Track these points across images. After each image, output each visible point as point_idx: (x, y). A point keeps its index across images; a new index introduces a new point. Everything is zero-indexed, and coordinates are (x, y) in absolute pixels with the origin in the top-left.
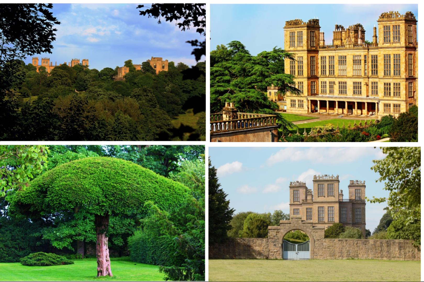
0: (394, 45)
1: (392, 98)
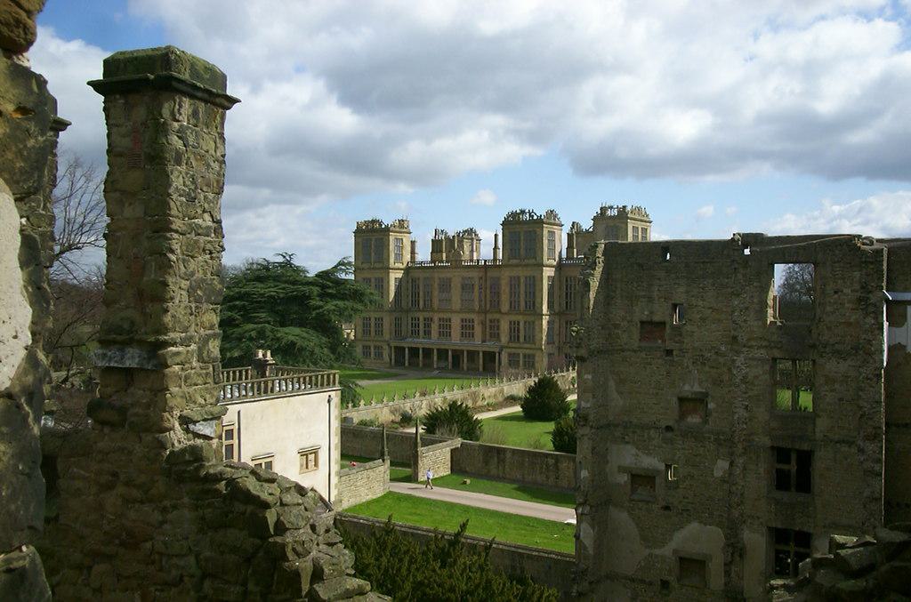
1: (522, 346)
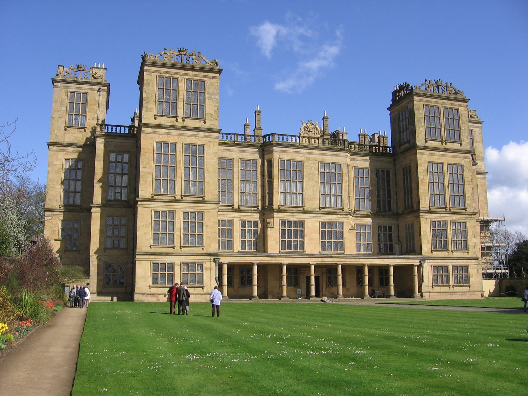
0: (449, 145)
1: (450, 255)
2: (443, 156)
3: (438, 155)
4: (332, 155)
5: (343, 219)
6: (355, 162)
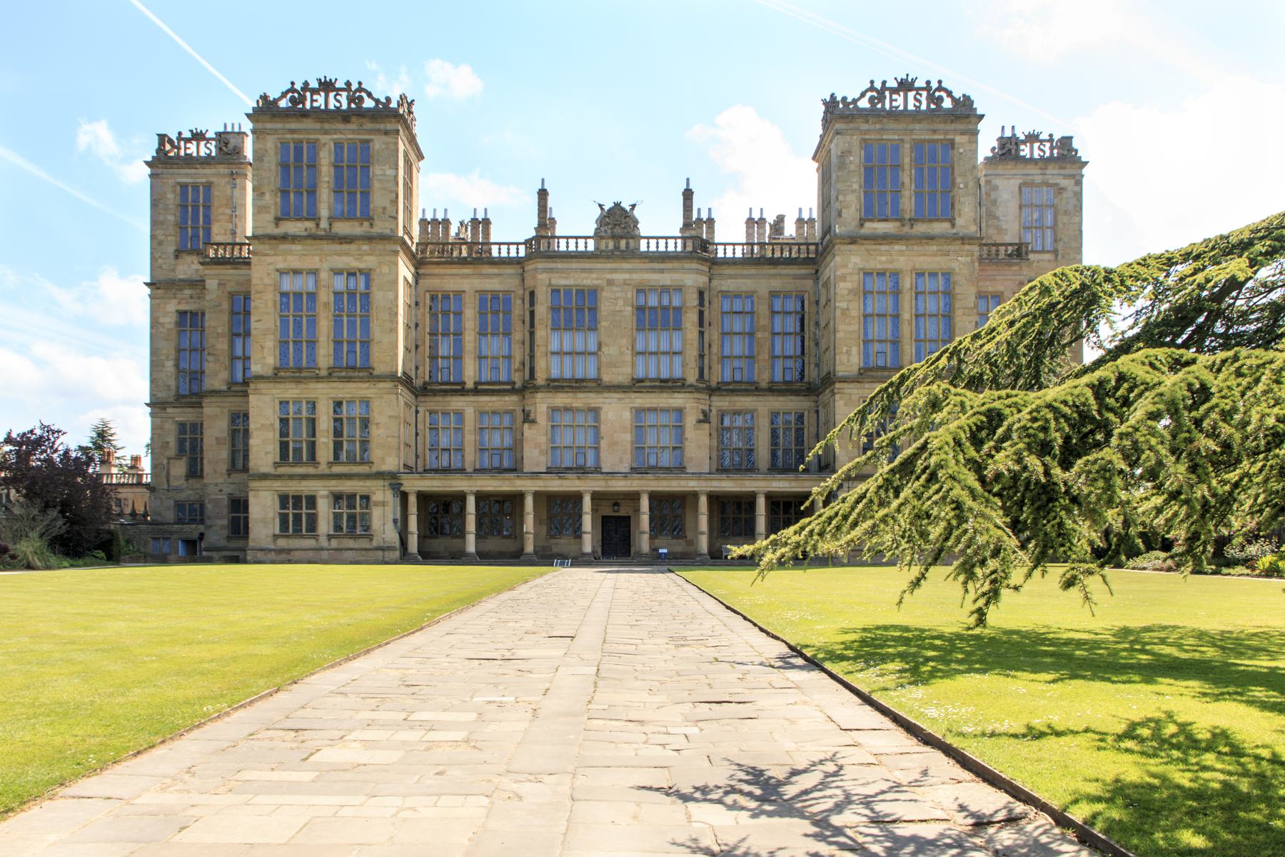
2: (901, 253)
3: (889, 253)
4: (662, 271)
5: (680, 401)
6: (723, 282)
